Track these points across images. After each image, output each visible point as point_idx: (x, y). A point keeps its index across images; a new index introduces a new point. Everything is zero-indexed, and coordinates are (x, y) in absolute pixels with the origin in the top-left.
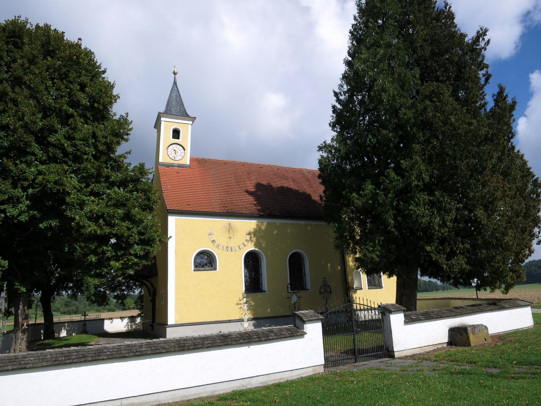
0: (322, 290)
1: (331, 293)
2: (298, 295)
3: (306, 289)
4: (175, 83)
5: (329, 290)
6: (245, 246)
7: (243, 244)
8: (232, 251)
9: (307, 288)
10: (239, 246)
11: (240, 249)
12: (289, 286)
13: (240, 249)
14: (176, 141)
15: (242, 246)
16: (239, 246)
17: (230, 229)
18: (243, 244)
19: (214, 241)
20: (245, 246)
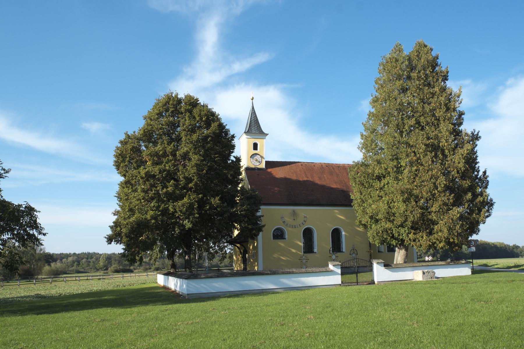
0: (352, 253)
1: (357, 254)
2: (336, 255)
3: (342, 252)
4: (253, 108)
5: (356, 252)
6: (303, 224)
7: (302, 223)
8: (295, 228)
9: (343, 251)
10: (300, 225)
11: (300, 226)
12: (331, 250)
13: (300, 226)
14: (255, 152)
15: (301, 225)
16: (300, 225)
17: (294, 214)
18: (302, 223)
19: (285, 221)
20: (303, 224)
